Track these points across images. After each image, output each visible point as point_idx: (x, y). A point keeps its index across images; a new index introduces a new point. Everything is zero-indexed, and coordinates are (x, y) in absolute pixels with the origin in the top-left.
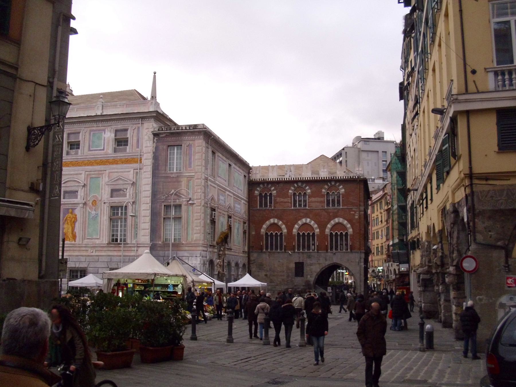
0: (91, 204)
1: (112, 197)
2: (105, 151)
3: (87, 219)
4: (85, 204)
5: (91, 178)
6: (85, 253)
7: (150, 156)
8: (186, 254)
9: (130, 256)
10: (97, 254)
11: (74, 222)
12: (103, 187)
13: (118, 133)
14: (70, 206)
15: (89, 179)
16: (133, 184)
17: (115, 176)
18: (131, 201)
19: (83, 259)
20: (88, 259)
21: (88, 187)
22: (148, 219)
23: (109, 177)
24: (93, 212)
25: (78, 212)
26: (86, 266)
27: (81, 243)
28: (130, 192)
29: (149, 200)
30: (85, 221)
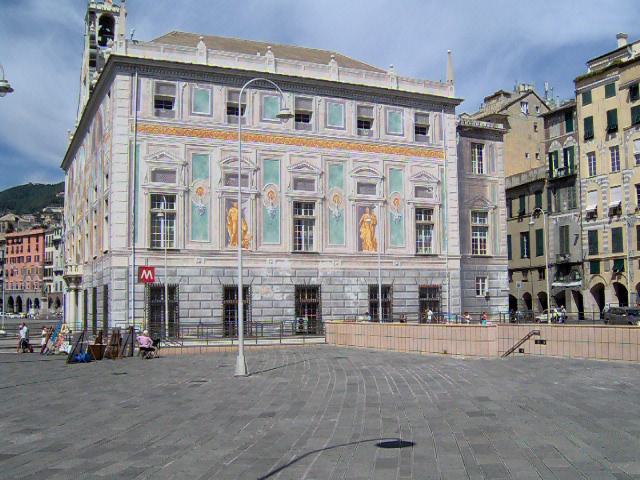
1: (416, 196)
6: (388, 266)
7: (454, 151)
8: (494, 268)
9: (439, 270)
10: (403, 267)
11: (374, 225)
13: (419, 118)
16: (439, 183)
17: (419, 170)
18: (184, 188)
19: (386, 274)
20: (392, 273)
22: (456, 227)
23: (411, 171)
26: (389, 283)
28: (435, 192)
29: (456, 204)
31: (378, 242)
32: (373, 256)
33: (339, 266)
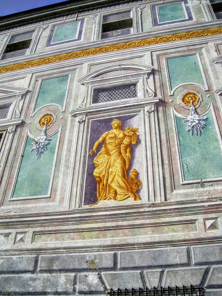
0: (179, 101)
2: (194, 19)
3: (174, 134)
4: (162, 103)
5: (167, 59)
6: (180, 234)
11: (131, 148)
12: (209, 68)
14: (114, 114)
15: (164, 62)
19: (176, 256)
21: (165, 73)
24: (192, 118)
25: (139, 123)
26: (195, 281)
27: (160, 199)
30: (168, 141)
31: (143, 178)
32: (134, 212)
33: (28, 245)
